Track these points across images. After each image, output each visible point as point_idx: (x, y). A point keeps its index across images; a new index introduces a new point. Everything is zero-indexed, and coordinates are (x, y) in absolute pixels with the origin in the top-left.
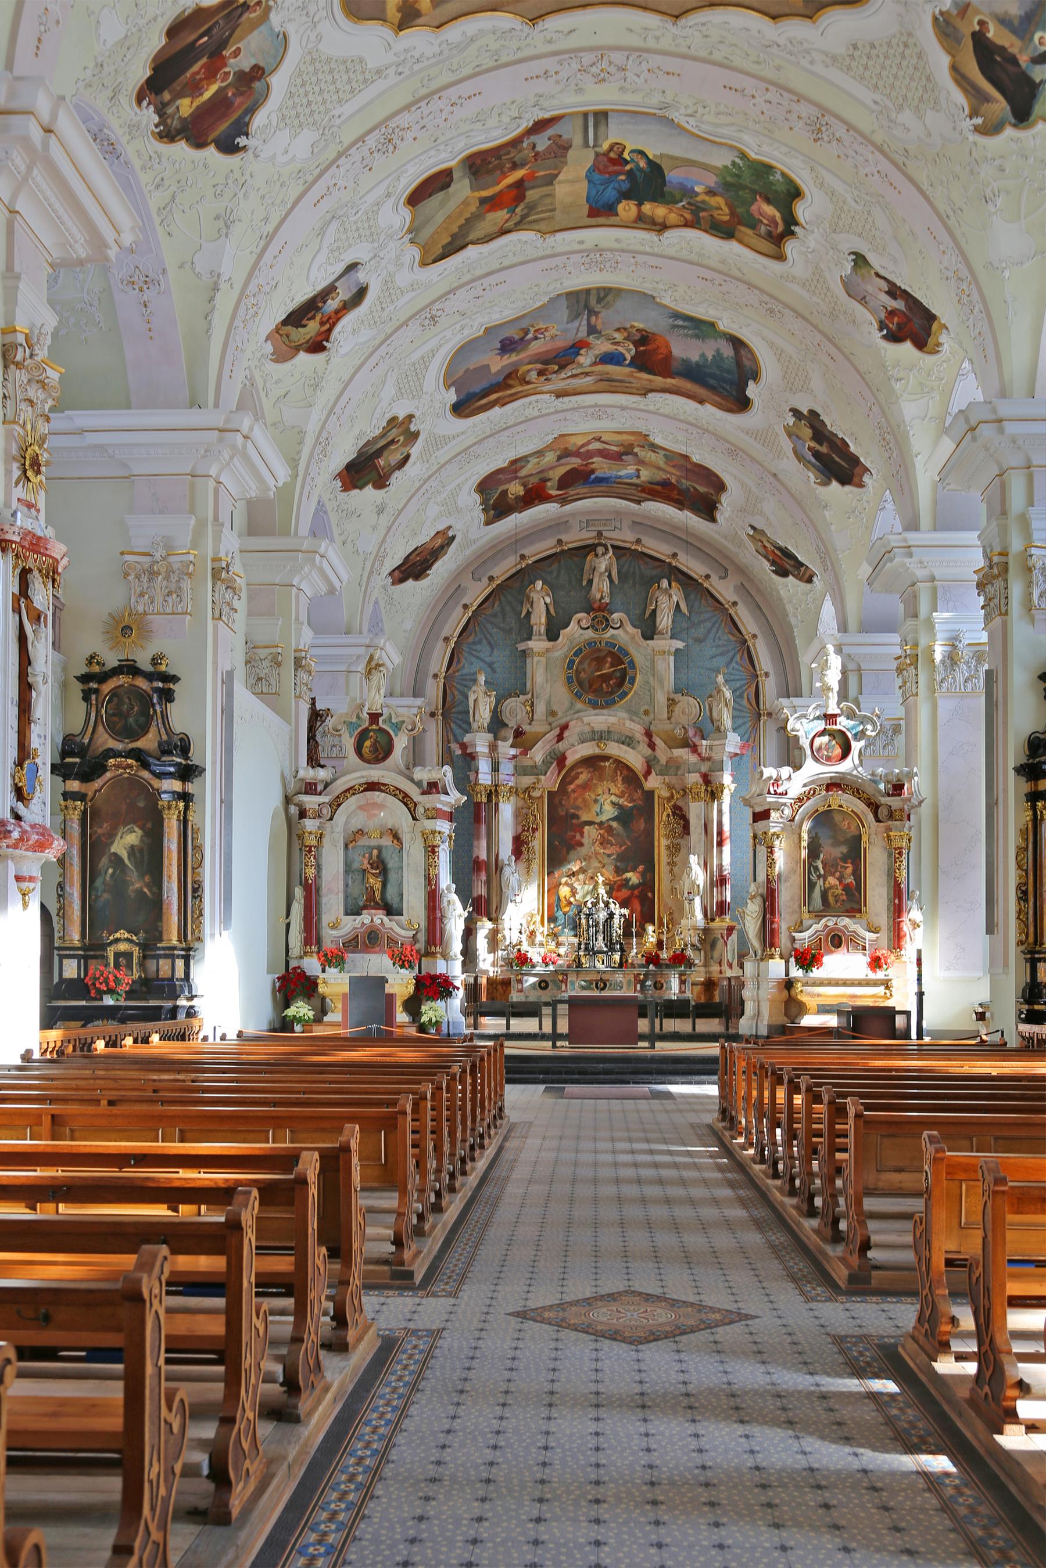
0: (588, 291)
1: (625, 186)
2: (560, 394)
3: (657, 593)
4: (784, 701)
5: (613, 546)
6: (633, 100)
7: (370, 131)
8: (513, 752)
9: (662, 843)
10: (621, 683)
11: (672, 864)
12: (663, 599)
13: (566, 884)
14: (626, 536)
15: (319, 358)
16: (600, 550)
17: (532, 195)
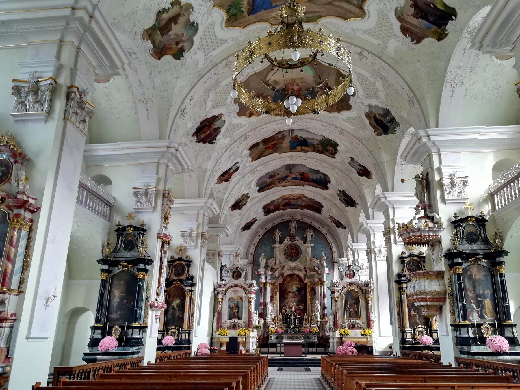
0: (290, 165)
1: (298, 144)
2: (283, 186)
4: (340, 259)
5: (296, 220)
6: (300, 127)
7: (241, 137)
8: (271, 273)
9: (309, 297)
10: (298, 255)
11: (311, 303)
12: (308, 233)
13: (284, 309)
14: (299, 218)
15: (228, 182)
16: (293, 221)
17: (277, 146)
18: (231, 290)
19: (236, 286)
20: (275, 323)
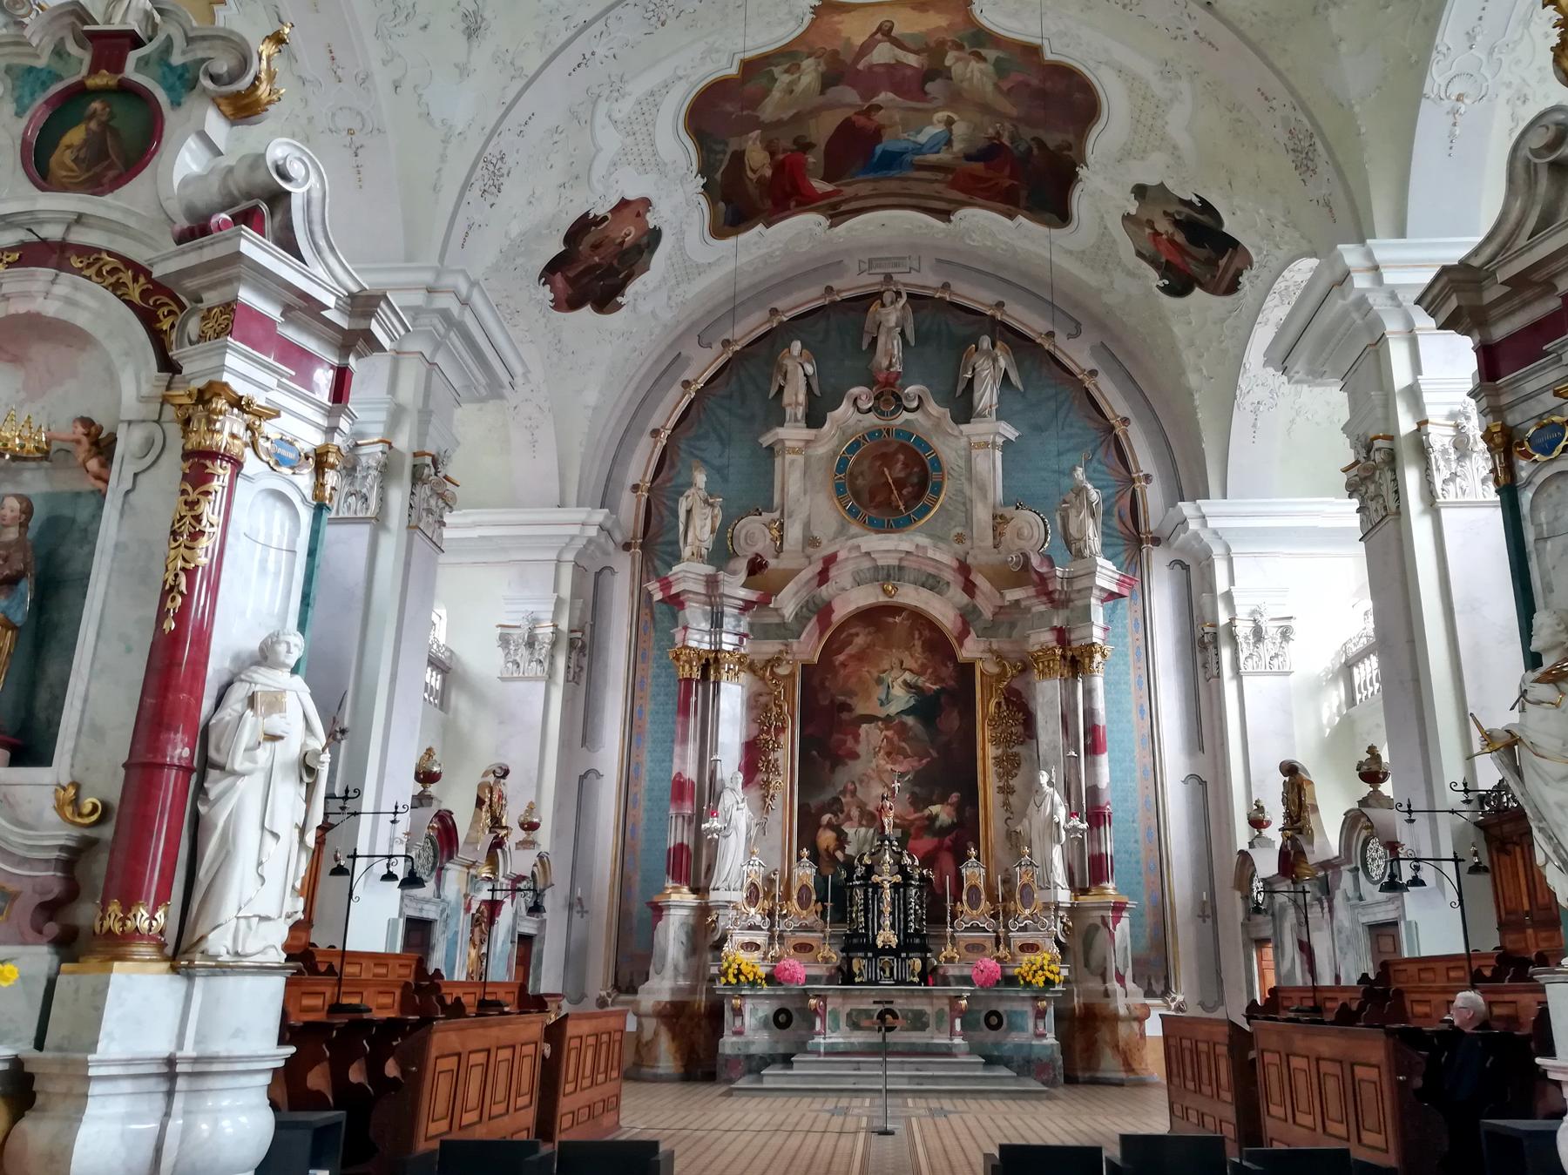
3: (975, 356)
5: (910, 296)
9: (988, 752)
10: (918, 494)
11: (1006, 790)
13: (830, 826)
14: (927, 280)
16: (888, 297)
20: (771, 914)
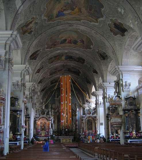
18: (41, 119)
19: (43, 117)
